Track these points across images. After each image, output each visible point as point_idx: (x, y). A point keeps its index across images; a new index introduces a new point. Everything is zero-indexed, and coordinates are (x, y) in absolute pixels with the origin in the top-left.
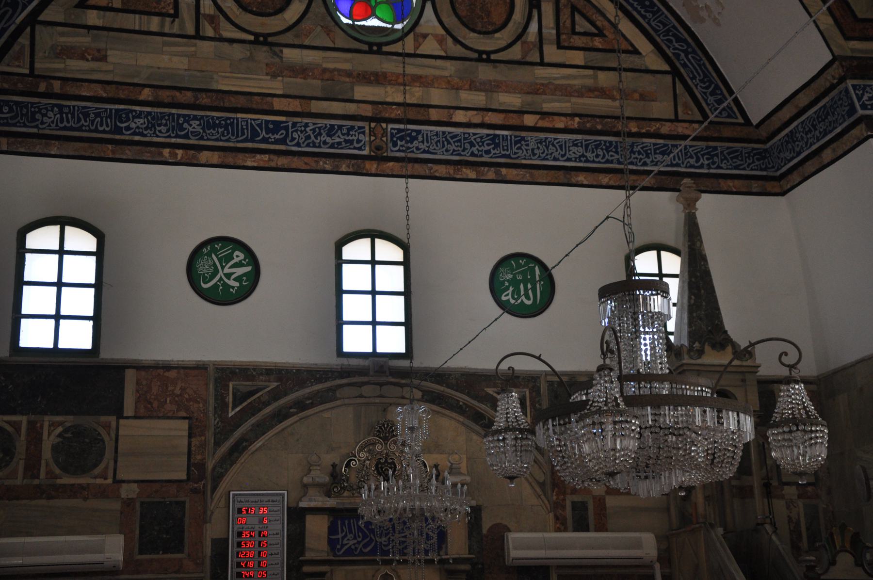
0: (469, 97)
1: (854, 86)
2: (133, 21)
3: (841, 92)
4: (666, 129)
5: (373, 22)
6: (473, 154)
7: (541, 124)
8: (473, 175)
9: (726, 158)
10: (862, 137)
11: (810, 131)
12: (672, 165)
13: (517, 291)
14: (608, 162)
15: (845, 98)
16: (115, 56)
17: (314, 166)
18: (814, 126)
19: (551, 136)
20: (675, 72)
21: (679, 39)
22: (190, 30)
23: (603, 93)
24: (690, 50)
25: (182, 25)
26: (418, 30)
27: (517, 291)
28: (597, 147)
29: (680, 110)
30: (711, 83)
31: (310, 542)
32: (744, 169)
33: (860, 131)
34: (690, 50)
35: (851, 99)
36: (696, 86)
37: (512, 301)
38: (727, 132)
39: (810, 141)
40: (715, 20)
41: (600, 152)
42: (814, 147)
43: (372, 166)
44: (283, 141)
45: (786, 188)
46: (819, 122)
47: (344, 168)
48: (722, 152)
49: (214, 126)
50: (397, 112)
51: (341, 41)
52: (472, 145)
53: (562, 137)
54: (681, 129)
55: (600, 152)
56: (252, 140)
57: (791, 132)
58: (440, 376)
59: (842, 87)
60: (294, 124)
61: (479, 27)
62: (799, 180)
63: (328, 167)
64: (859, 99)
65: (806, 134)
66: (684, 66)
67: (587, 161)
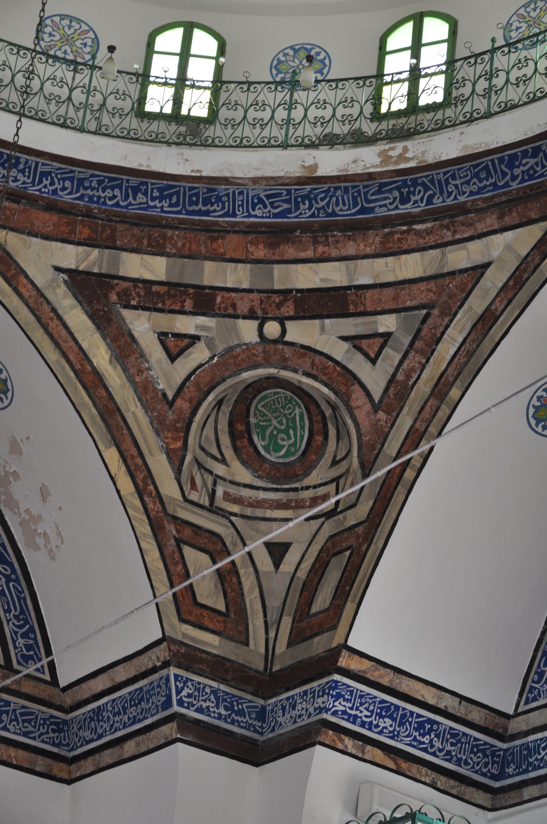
1: (176, 676)
3: (161, 678)
9: (16, 720)
10: (170, 738)
11: (119, 713)
15: (163, 686)
18: (124, 709)
24: (13, 577)
30: (26, 622)
32: (34, 738)
33: (170, 730)
34: (13, 577)
35: (170, 690)
36: (8, 621)
38: (28, 688)
39: (116, 725)
40: (50, 551)
42: (119, 734)
45: (74, 776)
46: (131, 706)
48: (14, 711)
57: (99, 707)
59: (164, 672)
62: (91, 769)
64: (178, 692)
65: (114, 716)
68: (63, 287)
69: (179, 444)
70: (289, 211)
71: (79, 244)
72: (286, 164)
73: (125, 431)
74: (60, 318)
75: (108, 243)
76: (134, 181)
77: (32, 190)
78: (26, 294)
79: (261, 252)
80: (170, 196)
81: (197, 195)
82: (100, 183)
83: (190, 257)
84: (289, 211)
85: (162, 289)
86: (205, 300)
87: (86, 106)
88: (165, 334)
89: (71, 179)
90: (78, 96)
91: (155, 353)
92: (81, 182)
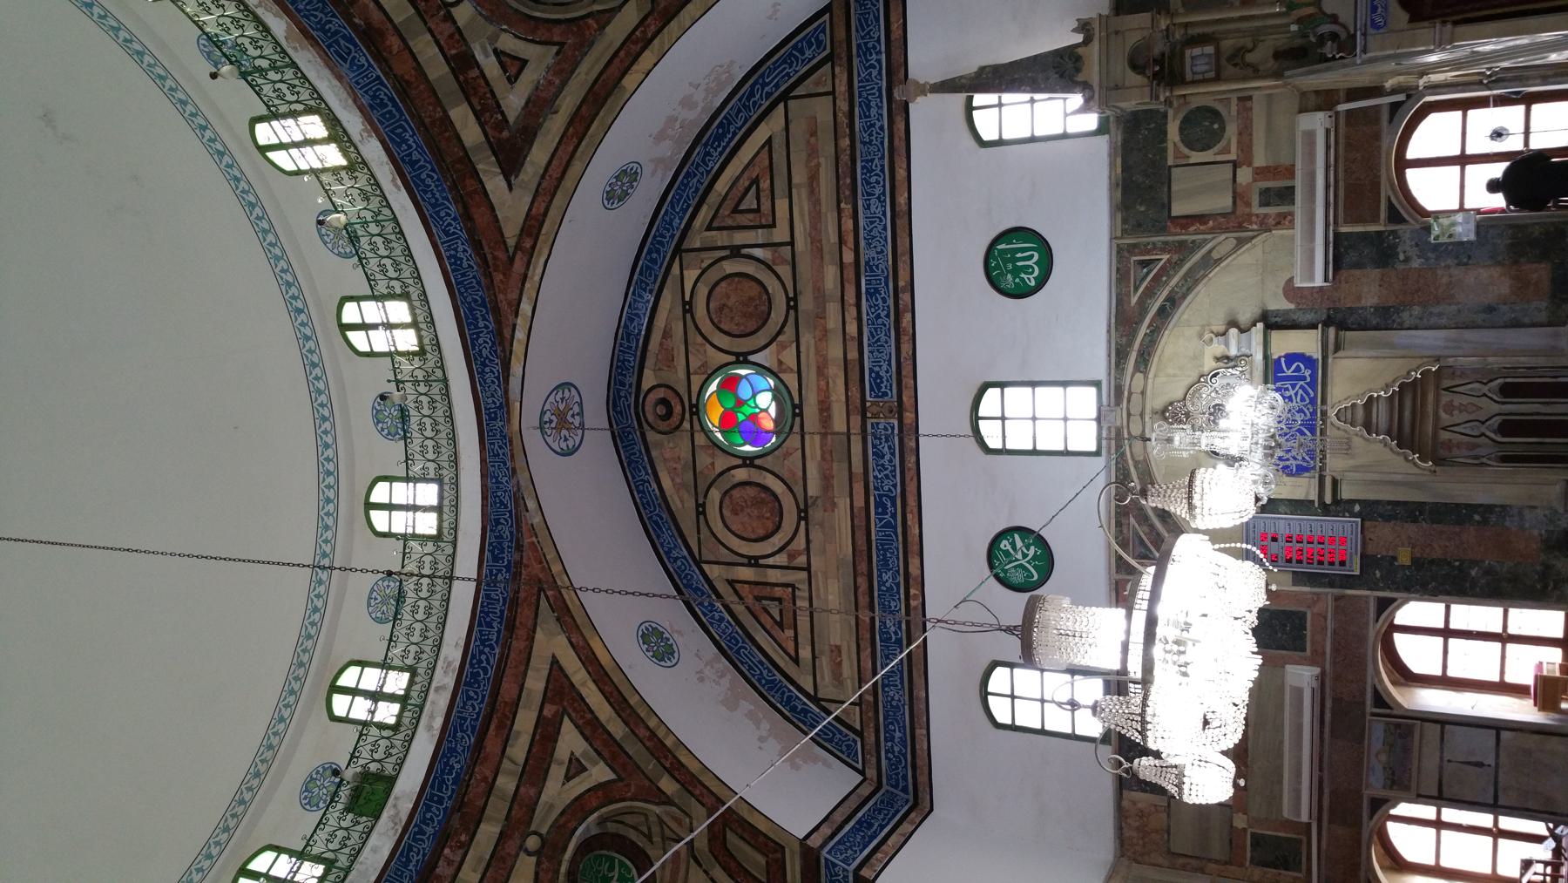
0: (833, 321)
2: (803, 621)
4: (843, 106)
5: (773, 411)
6: (888, 316)
7: (851, 243)
8: (908, 316)
12: (880, 96)
13: (1026, 269)
14: (882, 171)
16: (836, 640)
17: (913, 472)
19: (862, 233)
20: (785, 97)
21: (752, 94)
22: (804, 575)
23: (813, 178)
25: (800, 581)
26: (775, 369)
27: (1026, 269)
28: (868, 183)
29: (822, 90)
30: (791, 55)
31: (1299, 495)
37: (1036, 273)
38: (841, 34)
41: (873, 179)
43: (908, 417)
44: (893, 500)
47: (913, 444)
49: (885, 560)
50: (855, 392)
51: (794, 441)
52: (878, 317)
53: (861, 224)
54: (842, 88)
55: (873, 179)
56: (895, 527)
58: (1119, 355)
60: (876, 489)
61: (765, 308)
63: (913, 459)
66: (777, 86)
67: (884, 194)
68: (521, 176)
69: (590, 21)
70: (344, 37)
71: (481, 182)
72: (308, 60)
73: (604, 77)
74: (546, 170)
75: (466, 159)
76: (406, 169)
77: (464, 235)
78: (544, 205)
79: (394, 42)
80: (398, 135)
81: (383, 115)
82: (425, 192)
83: (435, 93)
84: (344, 37)
85: (475, 101)
86: (462, 63)
87: (377, 222)
88: (509, 79)
89: (437, 213)
90: (373, 229)
91: (529, 78)
92: (434, 206)
